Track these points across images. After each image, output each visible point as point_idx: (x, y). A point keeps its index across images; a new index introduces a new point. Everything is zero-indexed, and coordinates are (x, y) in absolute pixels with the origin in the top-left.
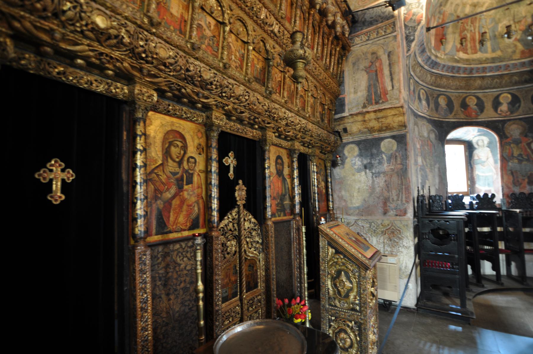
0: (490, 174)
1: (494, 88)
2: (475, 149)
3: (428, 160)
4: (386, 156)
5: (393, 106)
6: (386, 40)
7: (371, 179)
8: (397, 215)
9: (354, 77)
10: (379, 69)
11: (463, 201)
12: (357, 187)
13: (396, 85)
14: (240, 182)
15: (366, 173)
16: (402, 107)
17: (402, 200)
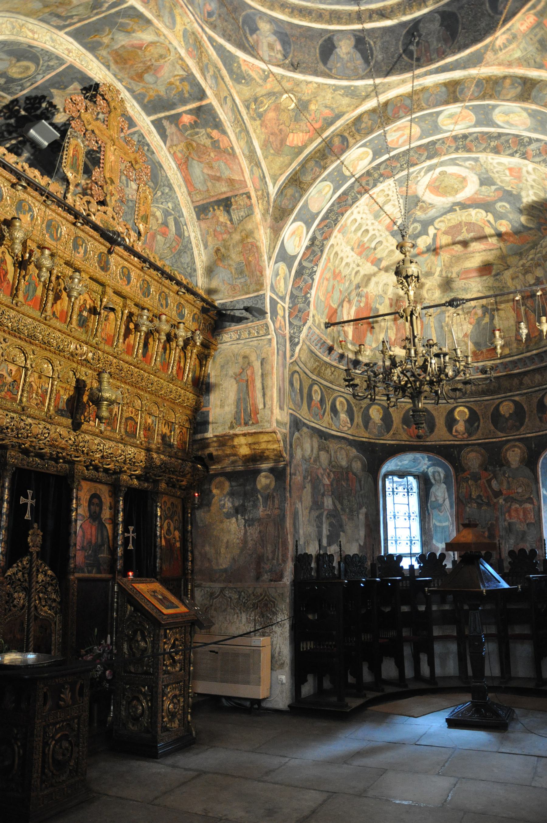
0: (446, 524)
2: (432, 485)
3: (345, 502)
4: (262, 496)
5: (264, 430)
6: (260, 342)
7: (243, 528)
8: (271, 580)
9: (221, 385)
10: (250, 379)
11: (401, 564)
12: (225, 541)
13: (269, 403)
14: (35, 525)
15: (237, 519)
17: (278, 559)
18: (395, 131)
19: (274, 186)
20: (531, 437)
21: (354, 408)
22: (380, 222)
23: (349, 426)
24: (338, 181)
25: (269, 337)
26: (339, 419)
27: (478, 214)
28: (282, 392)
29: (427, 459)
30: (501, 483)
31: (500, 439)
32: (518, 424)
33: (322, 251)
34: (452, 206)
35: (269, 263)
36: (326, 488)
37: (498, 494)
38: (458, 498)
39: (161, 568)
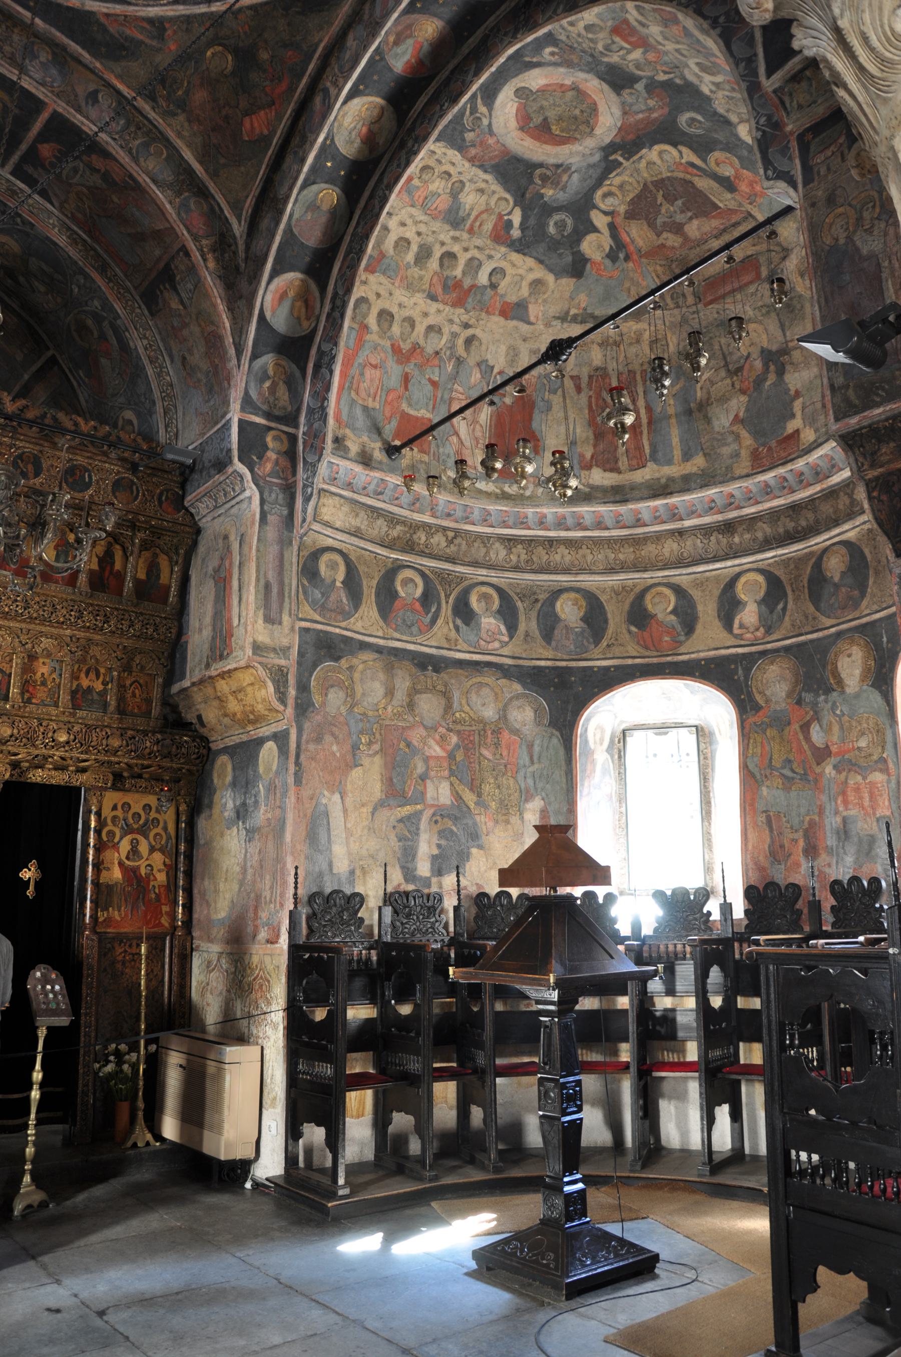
1: (715, 559)
8: (269, 941)
13: (244, 614)
16: (247, 667)
18: (396, 43)
19: (240, 222)
20: (881, 619)
21: (519, 604)
22: (471, 231)
23: (506, 639)
24: (348, 176)
25: (247, 493)
27: (665, 157)
28: (275, 590)
30: (828, 731)
31: (826, 632)
32: (856, 593)
33: (342, 316)
34: (606, 158)
35: (239, 360)
36: (432, 763)
39: (94, 917)
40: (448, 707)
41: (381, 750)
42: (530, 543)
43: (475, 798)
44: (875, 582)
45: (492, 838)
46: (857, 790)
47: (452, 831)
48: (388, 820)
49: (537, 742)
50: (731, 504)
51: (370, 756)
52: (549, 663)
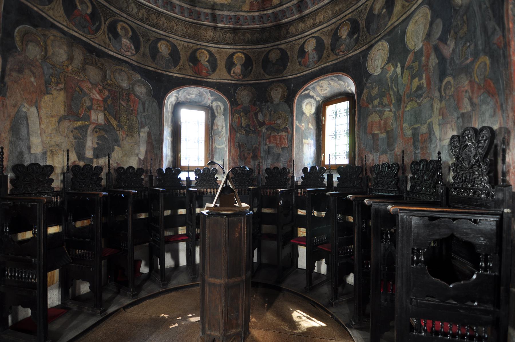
3: (123, 119)
20: (291, 78)
21: (141, 38)
23: (134, 53)
26: (120, 42)
29: (209, 94)
37: (262, 124)
38: (231, 126)
40: (104, 76)
41: (65, 88)
42: (149, 10)
43: (117, 123)
44: (291, 65)
45: (125, 142)
46: (275, 137)
47: (105, 137)
48: (68, 127)
49: (147, 103)
50: (238, 22)
51: (58, 90)
52: (153, 69)
